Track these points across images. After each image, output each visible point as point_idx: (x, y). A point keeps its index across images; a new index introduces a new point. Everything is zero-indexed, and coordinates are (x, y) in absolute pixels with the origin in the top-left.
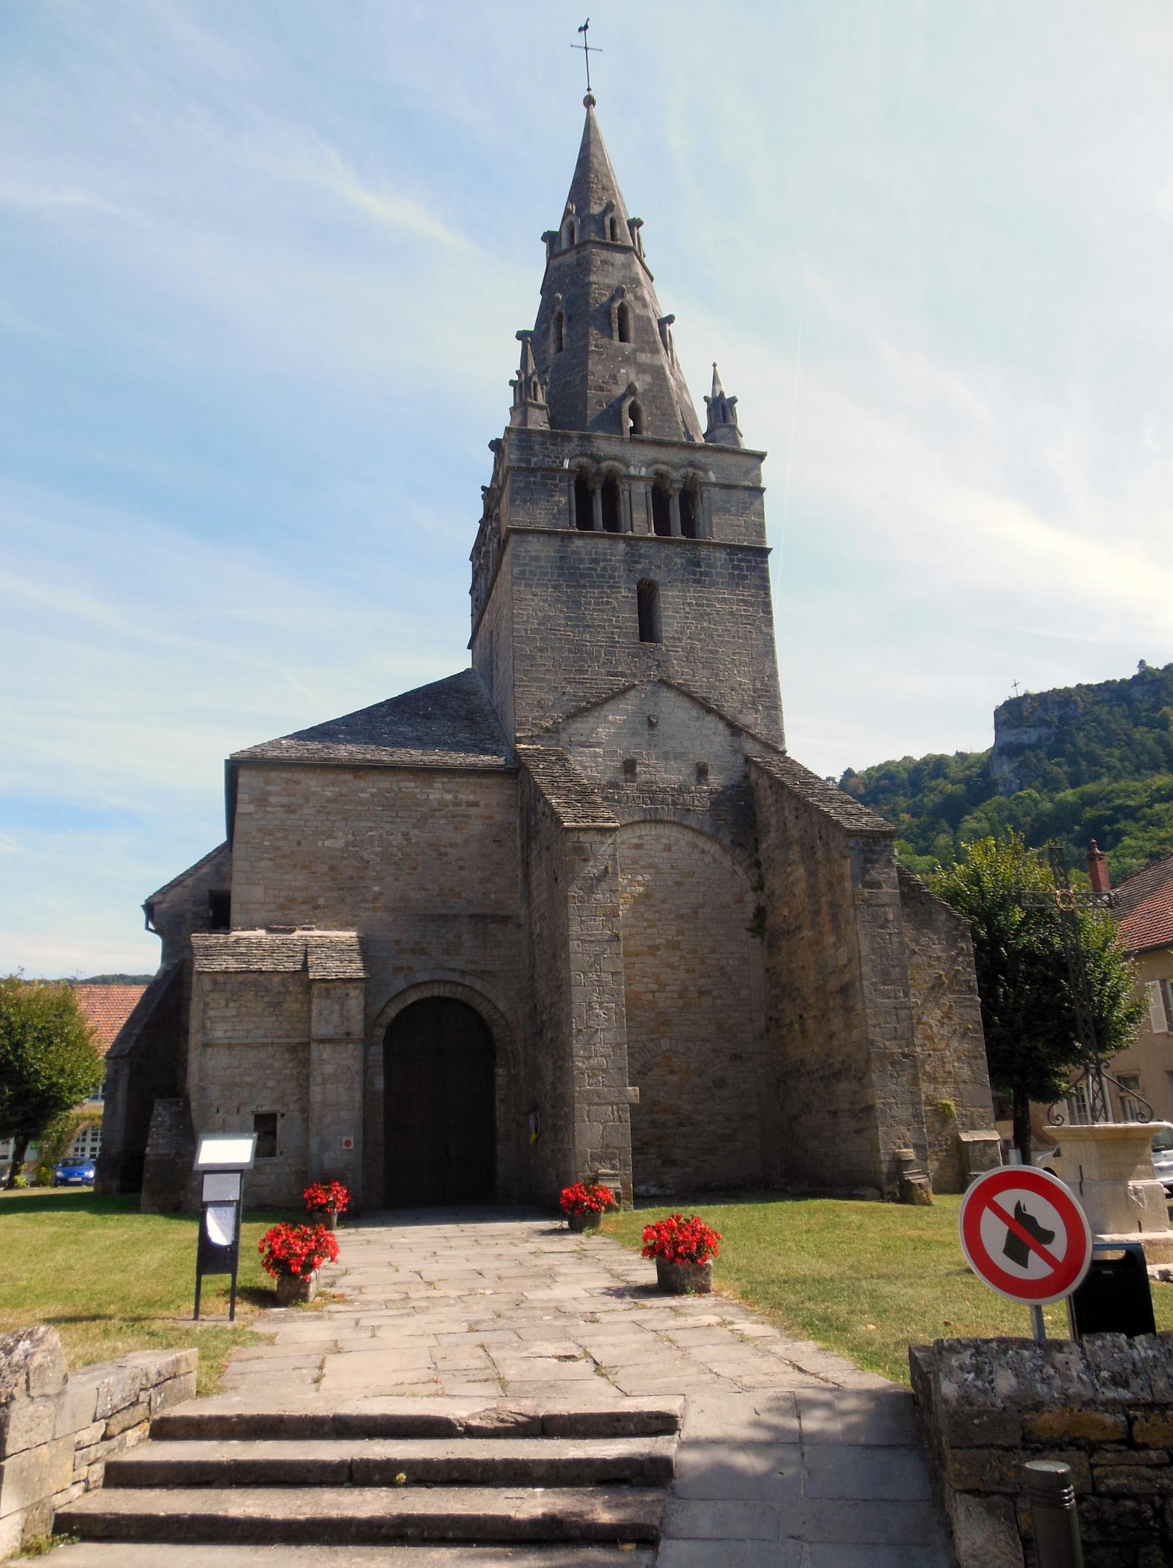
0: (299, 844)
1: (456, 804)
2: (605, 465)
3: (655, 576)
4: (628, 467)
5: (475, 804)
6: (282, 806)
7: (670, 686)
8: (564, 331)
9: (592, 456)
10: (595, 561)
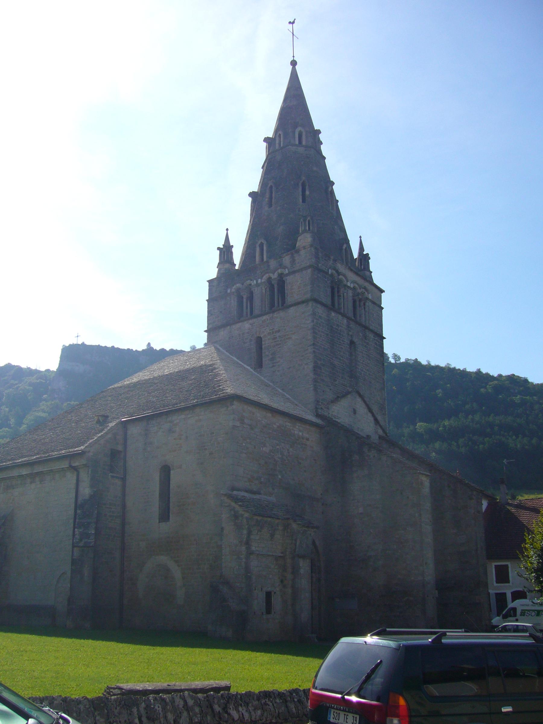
0: (255, 447)
1: (303, 438)
2: (341, 277)
3: (355, 340)
4: (347, 281)
5: (308, 439)
6: (249, 425)
7: (360, 396)
8: (307, 193)
9: (337, 271)
10: (338, 325)
